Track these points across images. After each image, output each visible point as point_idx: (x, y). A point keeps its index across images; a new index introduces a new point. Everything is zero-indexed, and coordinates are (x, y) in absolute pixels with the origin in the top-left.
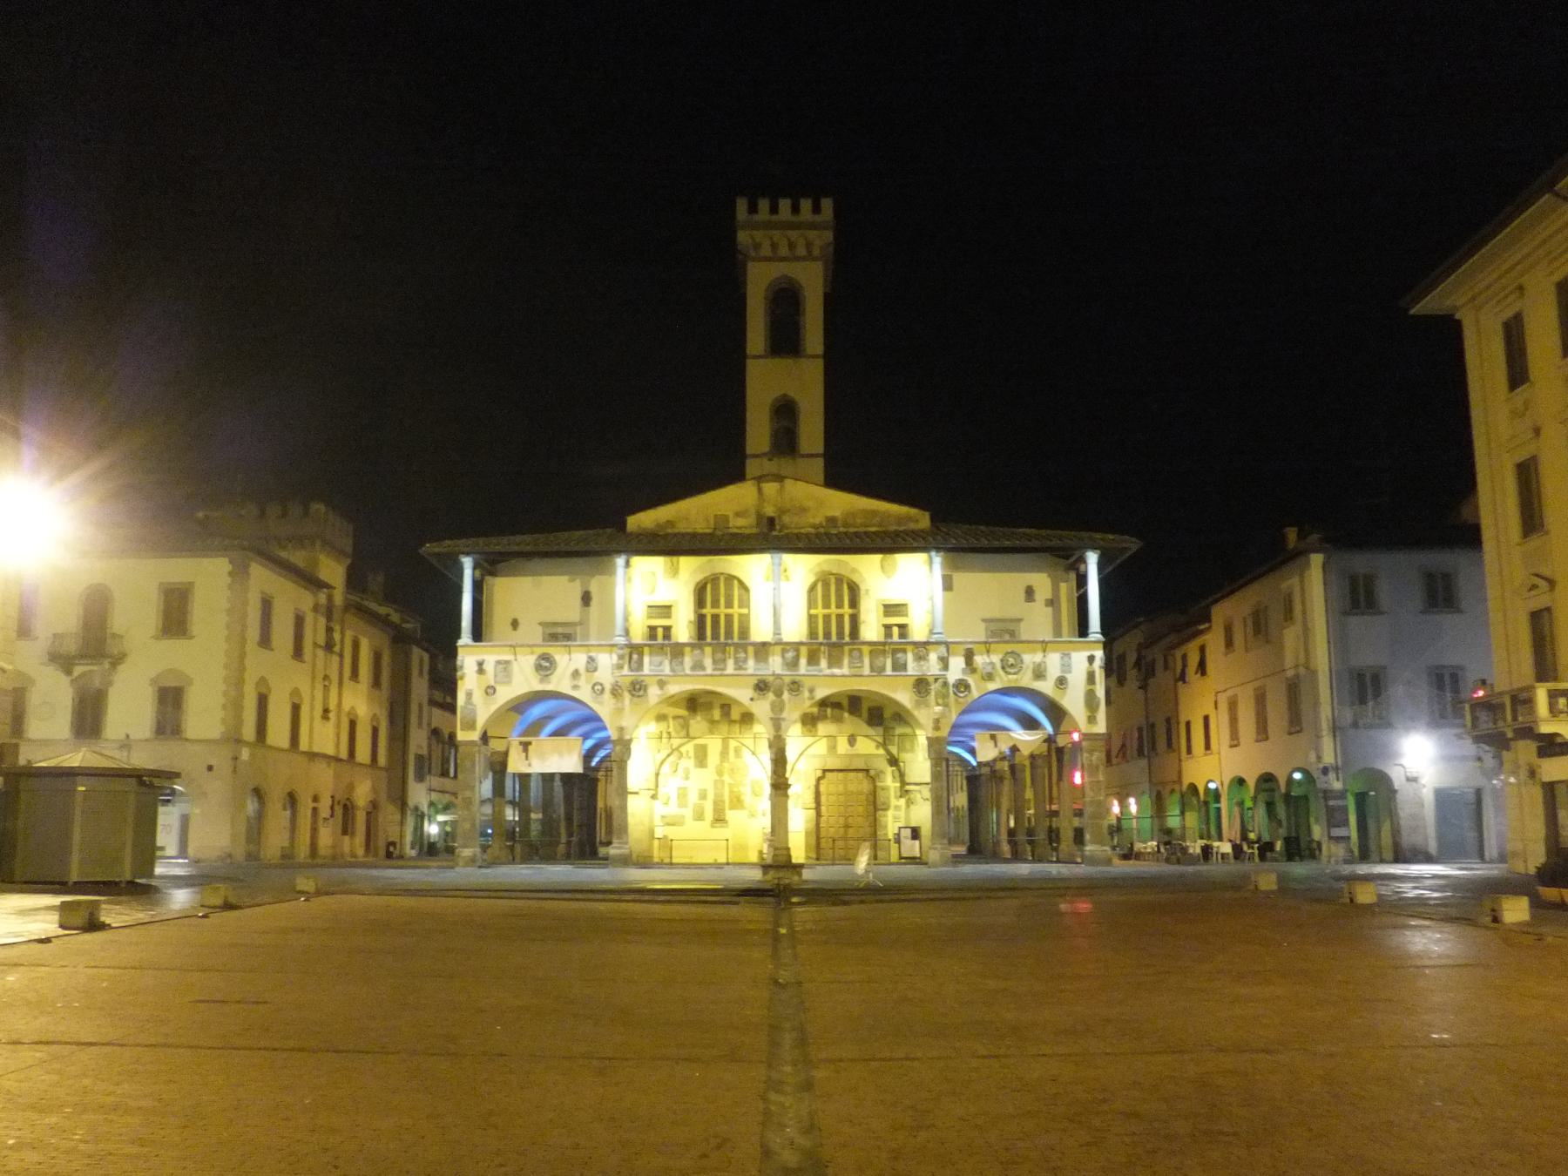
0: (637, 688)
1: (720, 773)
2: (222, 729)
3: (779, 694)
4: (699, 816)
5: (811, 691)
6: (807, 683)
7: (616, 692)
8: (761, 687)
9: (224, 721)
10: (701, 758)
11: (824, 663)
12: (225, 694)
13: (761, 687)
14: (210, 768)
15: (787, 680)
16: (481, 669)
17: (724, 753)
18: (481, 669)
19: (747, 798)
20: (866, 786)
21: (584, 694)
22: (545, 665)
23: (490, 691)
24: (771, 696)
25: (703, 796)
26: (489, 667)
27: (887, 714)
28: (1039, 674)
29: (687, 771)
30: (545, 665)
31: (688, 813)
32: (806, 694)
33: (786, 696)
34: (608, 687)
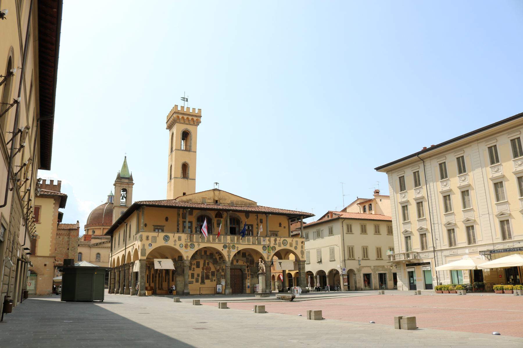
0: (192, 246)
1: (203, 269)
2: (50, 253)
3: (229, 249)
4: (197, 281)
5: (238, 248)
6: (236, 246)
7: (186, 246)
8: (225, 247)
9: (50, 250)
10: (198, 266)
11: (241, 241)
12: (51, 242)
13: (225, 247)
14: (45, 265)
15: (231, 245)
16: (147, 238)
17: (204, 264)
18: (147, 238)
19: (210, 277)
20: (240, 273)
21: (177, 247)
22: (166, 238)
23: (150, 245)
24: (227, 249)
25: (198, 275)
26: (150, 238)
27: (247, 255)
28: (291, 245)
29: (194, 269)
30: (166, 238)
31: (194, 280)
32: (236, 249)
33: (231, 249)
34: (184, 245)
